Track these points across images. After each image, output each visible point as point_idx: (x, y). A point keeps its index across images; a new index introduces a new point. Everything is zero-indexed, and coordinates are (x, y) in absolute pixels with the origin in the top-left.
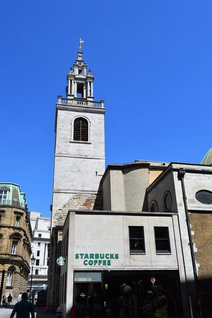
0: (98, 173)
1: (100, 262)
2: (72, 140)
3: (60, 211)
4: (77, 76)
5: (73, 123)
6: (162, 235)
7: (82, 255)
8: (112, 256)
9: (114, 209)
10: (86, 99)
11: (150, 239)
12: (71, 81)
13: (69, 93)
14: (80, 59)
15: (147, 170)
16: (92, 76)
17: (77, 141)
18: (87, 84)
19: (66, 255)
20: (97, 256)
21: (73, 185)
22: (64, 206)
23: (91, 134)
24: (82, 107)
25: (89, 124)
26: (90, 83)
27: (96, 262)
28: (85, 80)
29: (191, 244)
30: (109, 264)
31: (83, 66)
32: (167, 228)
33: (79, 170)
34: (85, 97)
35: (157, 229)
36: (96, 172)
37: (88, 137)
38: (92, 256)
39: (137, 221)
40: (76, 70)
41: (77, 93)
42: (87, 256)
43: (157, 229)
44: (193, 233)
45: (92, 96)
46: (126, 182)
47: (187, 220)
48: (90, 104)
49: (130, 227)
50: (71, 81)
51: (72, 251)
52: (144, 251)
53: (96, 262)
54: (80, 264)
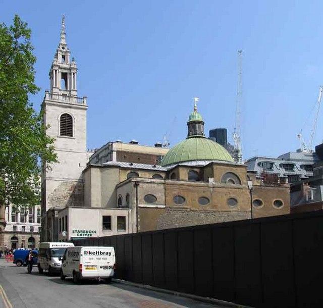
0: (81, 166)
1: (86, 235)
2: (59, 135)
3: (52, 194)
4: (61, 65)
5: (59, 119)
6: (121, 220)
7: (76, 231)
8: (92, 232)
9: (93, 205)
10: (70, 91)
11: (114, 223)
12: (56, 71)
13: (54, 86)
14: (63, 42)
15: (118, 169)
16: (75, 67)
17: (63, 136)
18: (71, 74)
19: (67, 230)
20: (84, 231)
21: (61, 174)
22: (55, 191)
23: (75, 130)
24: (67, 103)
25: (73, 120)
26: (74, 74)
27: (84, 235)
28: (70, 69)
29: (137, 226)
30: (91, 235)
31: (67, 52)
32: (125, 217)
33: (66, 162)
34: (68, 89)
35: (119, 217)
36: (79, 164)
37: (72, 132)
38: (82, 231)
39: (108, 212)
40: (60, 56)
41: (62, 78)
42: (79, 231)
43: (119, 217)
44: (139, 220)
45: (75, 89)
46: (102, 178)
47: (137, 213)
48: (74, 101)
49: (103, 216)
50: (56, 71)
51: (71, 229)
52: (111, 229)
53: (84, 235)
54: (75, 235)
